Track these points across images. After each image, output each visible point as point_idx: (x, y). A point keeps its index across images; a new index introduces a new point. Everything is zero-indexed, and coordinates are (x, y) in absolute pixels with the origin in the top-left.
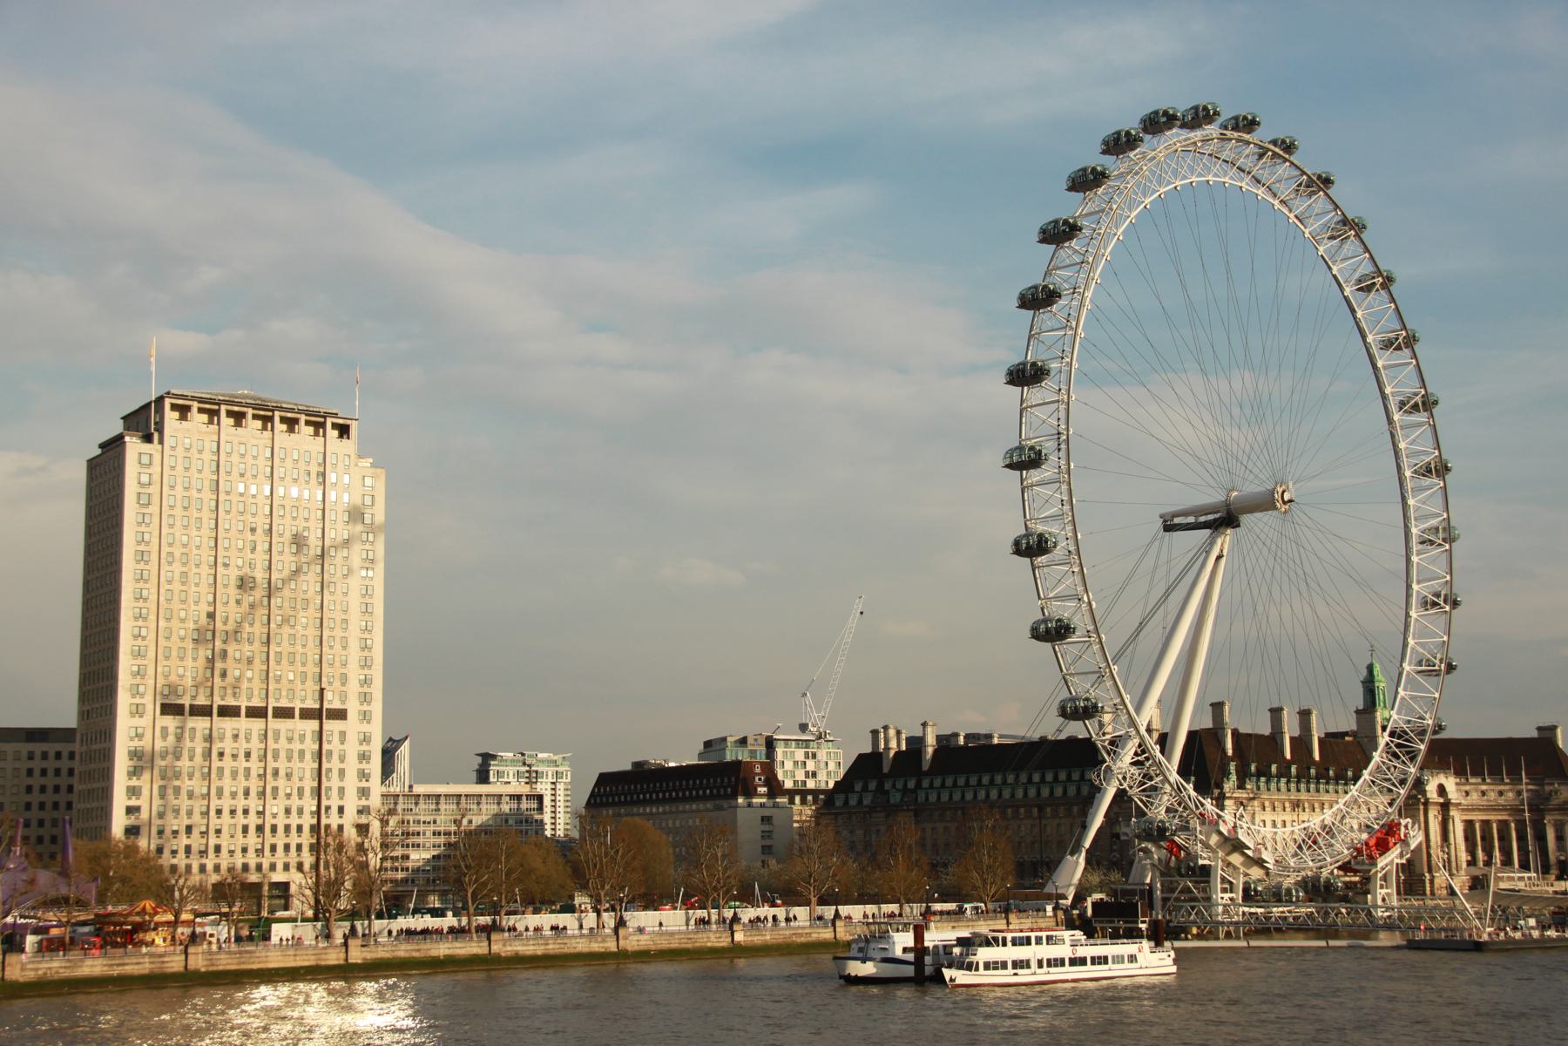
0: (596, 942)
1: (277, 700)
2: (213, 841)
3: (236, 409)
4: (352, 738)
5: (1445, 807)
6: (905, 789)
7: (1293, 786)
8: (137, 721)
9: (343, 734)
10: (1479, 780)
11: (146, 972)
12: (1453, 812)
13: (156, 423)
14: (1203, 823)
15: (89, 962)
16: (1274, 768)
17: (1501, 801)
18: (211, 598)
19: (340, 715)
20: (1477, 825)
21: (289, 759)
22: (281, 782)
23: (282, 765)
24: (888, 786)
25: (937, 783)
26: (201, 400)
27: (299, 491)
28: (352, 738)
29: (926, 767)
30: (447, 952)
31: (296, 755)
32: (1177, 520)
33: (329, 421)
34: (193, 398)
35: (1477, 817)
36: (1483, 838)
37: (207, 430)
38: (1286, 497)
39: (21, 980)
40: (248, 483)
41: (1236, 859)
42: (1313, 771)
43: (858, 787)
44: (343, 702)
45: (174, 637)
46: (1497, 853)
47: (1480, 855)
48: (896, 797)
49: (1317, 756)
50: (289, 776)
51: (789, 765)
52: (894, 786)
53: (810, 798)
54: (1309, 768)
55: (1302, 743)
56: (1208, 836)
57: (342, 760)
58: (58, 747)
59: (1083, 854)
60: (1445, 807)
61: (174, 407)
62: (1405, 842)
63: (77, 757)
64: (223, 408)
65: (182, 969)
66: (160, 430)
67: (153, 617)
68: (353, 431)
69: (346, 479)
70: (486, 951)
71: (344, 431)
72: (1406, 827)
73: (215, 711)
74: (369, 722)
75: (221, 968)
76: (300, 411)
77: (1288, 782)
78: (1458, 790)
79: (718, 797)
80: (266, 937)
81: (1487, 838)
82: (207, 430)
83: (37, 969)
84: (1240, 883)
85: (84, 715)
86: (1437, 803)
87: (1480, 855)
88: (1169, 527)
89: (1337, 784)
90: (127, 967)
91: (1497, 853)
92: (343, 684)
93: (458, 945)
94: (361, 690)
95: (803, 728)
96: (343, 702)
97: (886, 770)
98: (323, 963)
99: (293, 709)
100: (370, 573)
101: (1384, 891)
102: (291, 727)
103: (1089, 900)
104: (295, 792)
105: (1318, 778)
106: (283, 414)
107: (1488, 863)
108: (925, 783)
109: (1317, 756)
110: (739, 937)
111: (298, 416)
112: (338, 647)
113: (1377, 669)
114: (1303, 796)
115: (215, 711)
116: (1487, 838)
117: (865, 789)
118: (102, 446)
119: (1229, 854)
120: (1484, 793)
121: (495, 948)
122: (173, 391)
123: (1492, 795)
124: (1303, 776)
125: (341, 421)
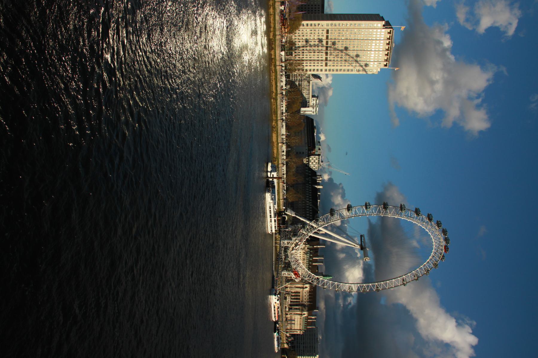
0: (280, 115)
2: (301, 41)
3: (390, 43)
4: (321, 68)
5: (303, 288)
6: (309, 181)
7: (308, 259)
8: (325, 25)
9: (322, 66)
10: (308, 295)
11: (276, 28)
12: (302, 289)
13: (387, 27)
14: (301, 239)
15: (278, 17)
16: (312, 255)
17: (304, 299)
18: (351, 39)
19: (326, 65)
20: (299, 294)
21: (318, 55)
22: (312, 54)
23: (316, 54)
24: (310, 178)
25: (310, 188)
26: (392, 36)
27: (373, 57)
28: (321, 68)
29: (313, 186)
30: (278, 85)
31: (318, 56)
32: (363, 238)
33: (388, 62)
34: (392, 35)
35: (301, 294)
36: (297, 295)
38: (367, 260)
39: (275, 5)
41: (293, 245)
42: (311, 263)
43: (310, 172)
45: (342, 32)
46: (294, 297)
47: (293, 294)
48: (307, 179)
49: (313, 264)
50: (314, 55)
51: (314, 159)
52: (310, 179)
53: (308, 162)
54: (311, 262)
55: (316, 261)
56: (298, 240)
58: (321, 10)
59: (295, 216)
60: (303, 288)
61: (391, 31)
62: (296, 278)
63: (318, 14)
64: (390, 41)
65: (276, 34)
66: (386, 28)
67: (347, 27)
68: (385, 67)
69: (375, 66)
70: (278, 93)
71: (386, 65)
72: (299, 279)
73: (327, 40)
75: (276, 42)
76: (390, 56)
77: (309, 258)
78: (306, 291)
79: (308, 143)
80: (282, 51)
81: (297, 296)
83: (277, 8)
84: (289, 245)
85: (327, 15)
86: (304, 286)
87: (293, 294)
88: (361, 236)
89: (308, 267)
90: (277, 24)
91: (294, 297)
93: (280, 87)
95: (322, 162)
97: (313, 178)
98: (277, 61)
99: (327, 55)
100: (356, 71)
101: (287, 274)
103: (286, 216)
104: (310, 56)
105: (309, 264)
106: (389, 53)
107: (292, 296)
108: (310, 185)
109: (313, 264)
110: (280, 144)
111: (389, 56)
112: (341, 64)
113: (331, 278)
114: (305, 261)
116: (297, 296)
117: (309, 173)
118: (382, 17)
119: (295, 244)
120: (305, 296)
121: (279, 95)
122: (394, 31)
123: (305, 297)
124: (310, 261)
125: (388, 65)
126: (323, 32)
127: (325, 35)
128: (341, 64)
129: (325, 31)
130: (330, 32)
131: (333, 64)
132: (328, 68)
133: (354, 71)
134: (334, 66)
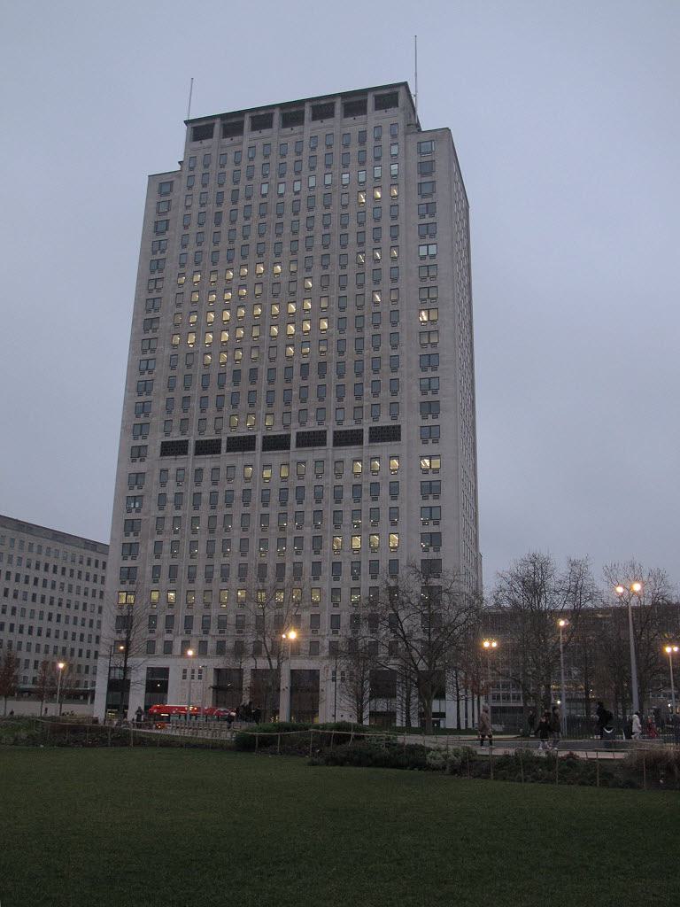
1: (302, 424)
37: (232, 142)
40: (273, 182)
44: (394, 418)
57: (394, 496)
73: (224, 445)
74: (436, 441)
82: (232, 142)
92: (394, 393)
94: (424, 399)
96: (394, 418)
102: (321, 457)
112: (386, 346)
115: (224, 445)
126: (172, 472)
127: (189, 462)
128: (386, 346)
129: (172, 464)
130: (176, 436)
131: (385, 394)
132: (411, 423)
133: (433, 256)
134: (395, 387)
